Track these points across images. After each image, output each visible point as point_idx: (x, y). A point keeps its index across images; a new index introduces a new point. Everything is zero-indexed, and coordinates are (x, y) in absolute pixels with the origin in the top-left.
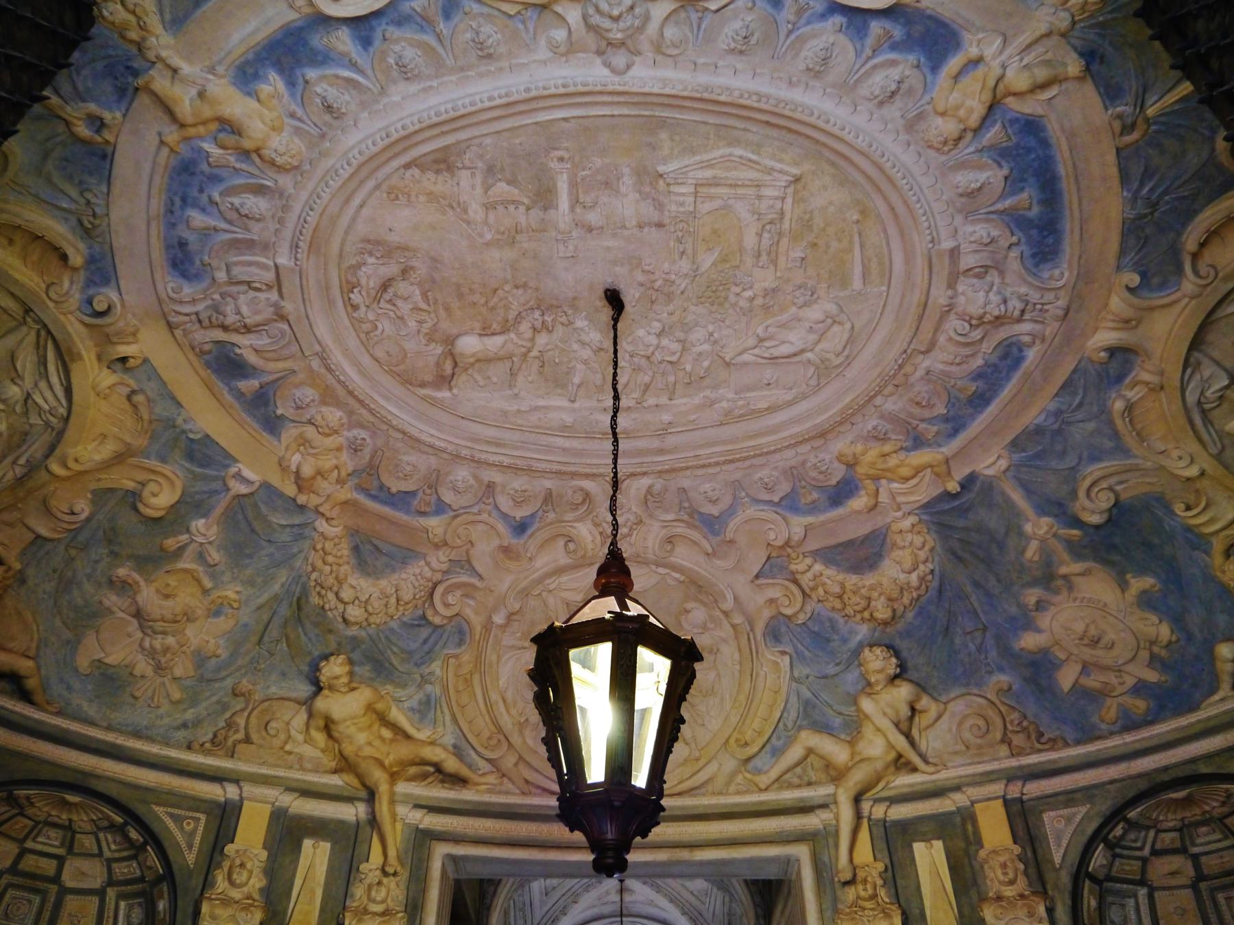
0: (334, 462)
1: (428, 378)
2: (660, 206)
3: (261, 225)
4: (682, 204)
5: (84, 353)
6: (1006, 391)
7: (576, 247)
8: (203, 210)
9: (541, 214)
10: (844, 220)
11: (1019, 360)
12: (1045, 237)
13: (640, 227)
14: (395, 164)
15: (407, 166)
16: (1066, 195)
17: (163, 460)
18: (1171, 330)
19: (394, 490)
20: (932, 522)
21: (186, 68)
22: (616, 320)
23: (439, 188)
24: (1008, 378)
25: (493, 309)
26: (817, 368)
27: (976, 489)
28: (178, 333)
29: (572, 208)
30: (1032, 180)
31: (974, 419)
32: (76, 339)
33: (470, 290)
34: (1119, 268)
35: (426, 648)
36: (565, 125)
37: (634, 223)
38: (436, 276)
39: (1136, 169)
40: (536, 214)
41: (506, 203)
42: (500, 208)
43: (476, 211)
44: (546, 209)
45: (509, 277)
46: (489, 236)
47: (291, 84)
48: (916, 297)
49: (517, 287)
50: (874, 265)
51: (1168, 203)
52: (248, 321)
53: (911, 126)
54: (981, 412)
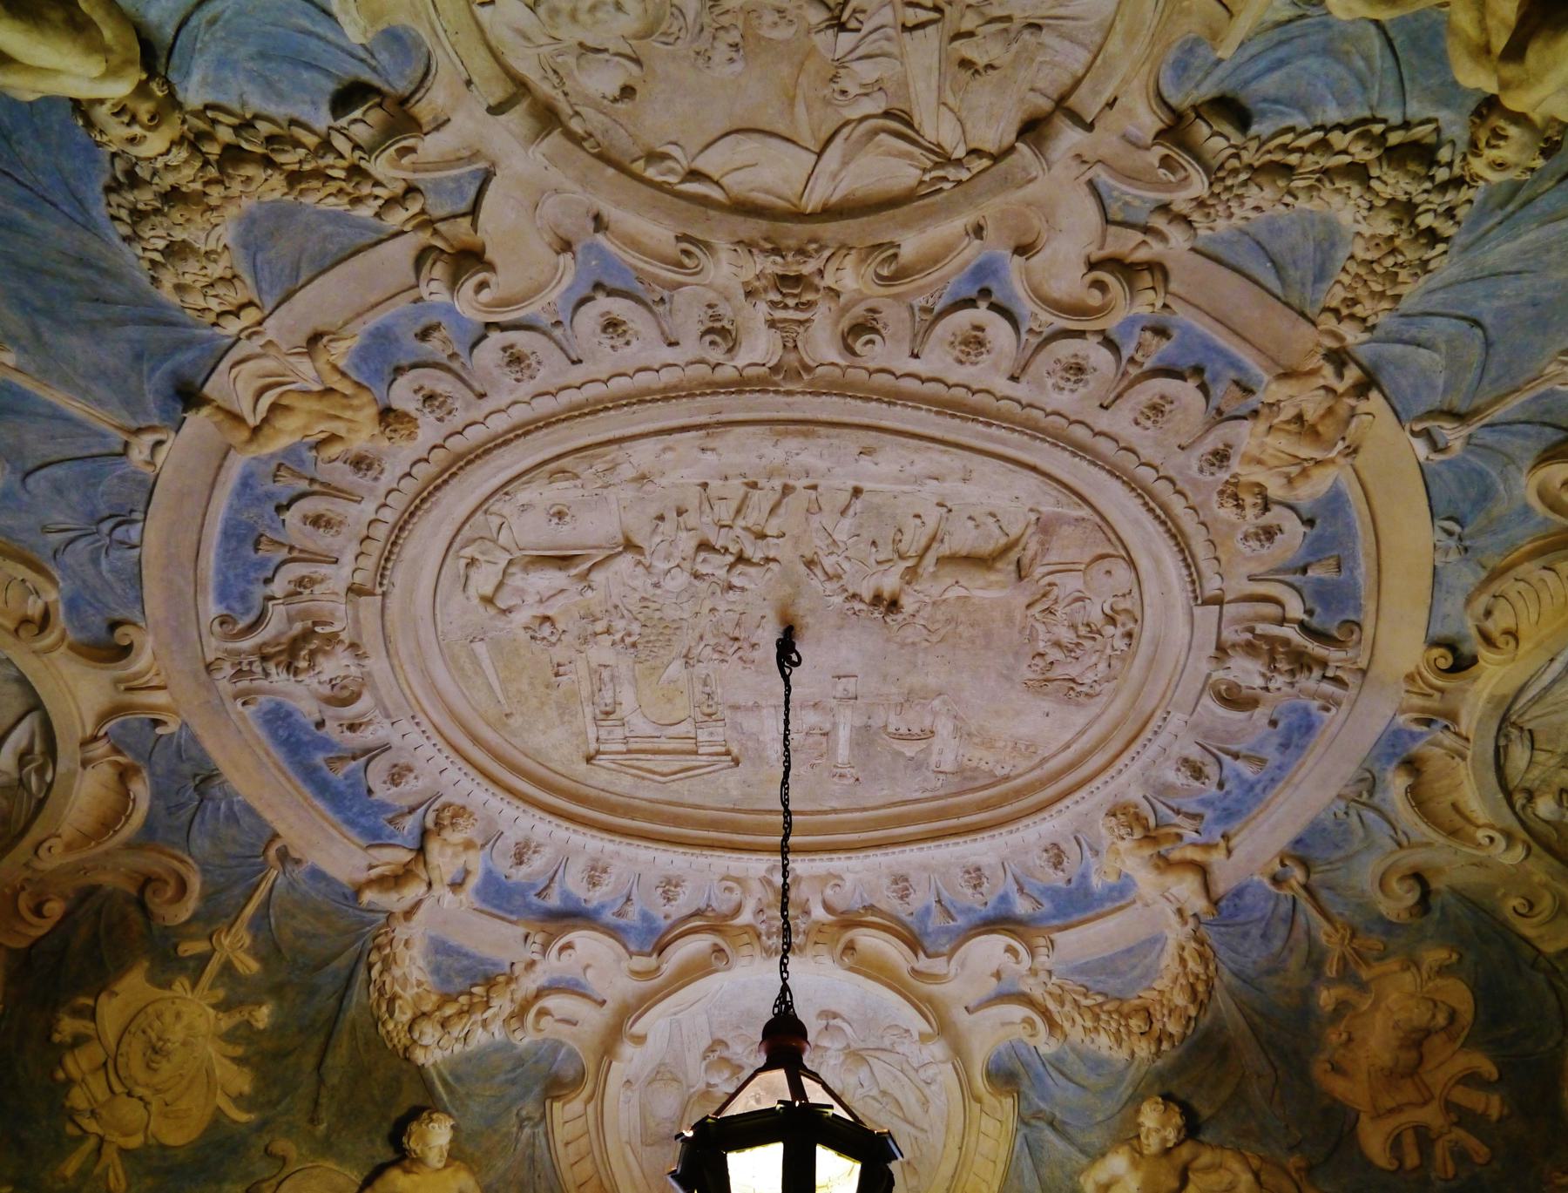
0: (1269, 440)
1: (1066, 530)
2: (736, 727)
3: (1185, 753)
4: (711, 734)
5: (1485, 695)
6: (212, 556)
7: (834, 686)
8: (1238, 775)
9: (871, 722)
10: (522, 714)
11: (223, 596)
12: (290, 735)
13: (757, 706)
14: (1019, 781)
15: (1007, 778)
16: (299, 783)
17: (1527, 510)
18: (74, 698)
19: (1191, 384)
20: (185, 325)
21: (1169, 910)
22: (785, 989)
23: (978, 753)
24: (219, 571)
25: (948, 621)
26: (495, 541)
27: (150, 397)
28: (1363, 663)
29: (835, 725)
30: (342, 788)
31: (231, 506)
32: (1477, 714)
33: (973, 642)
34: (184, 725)
35: (1281, 52)
36: (835, 804)
37: (765, 711)
38: (1012, 660)
39: (246, 821)
40: (877, 722)
41: (909, 737)
42: (915, 730)
43: (944, 727)
44: (867, 727)
45: (921, 655)
46: (936, 703)
47: (1084, 876)
48: (403, 647)
49: (913, 644)
50: (468, 666)
51: (191, 799)
52: (1263, 670)
53: (492, 838)
54: (227, 521)
